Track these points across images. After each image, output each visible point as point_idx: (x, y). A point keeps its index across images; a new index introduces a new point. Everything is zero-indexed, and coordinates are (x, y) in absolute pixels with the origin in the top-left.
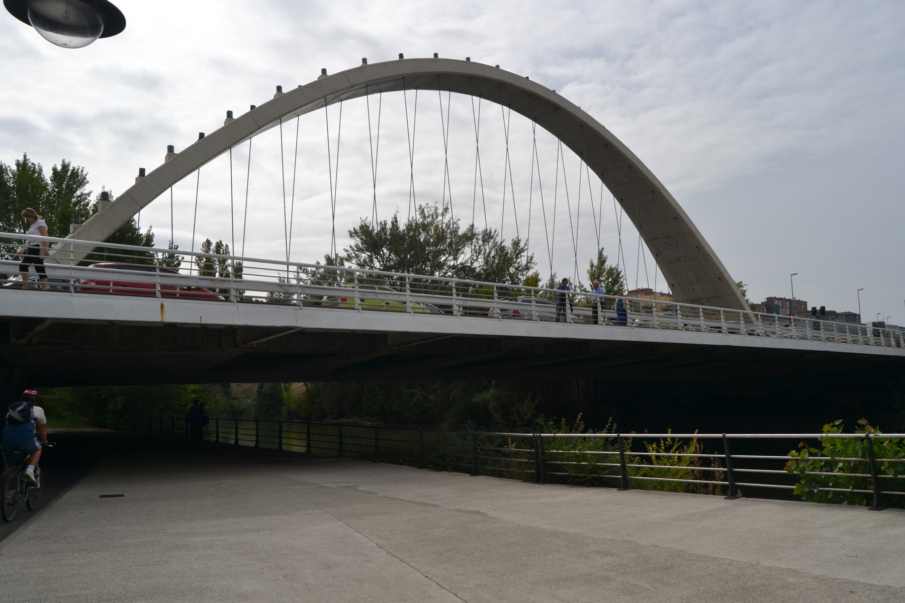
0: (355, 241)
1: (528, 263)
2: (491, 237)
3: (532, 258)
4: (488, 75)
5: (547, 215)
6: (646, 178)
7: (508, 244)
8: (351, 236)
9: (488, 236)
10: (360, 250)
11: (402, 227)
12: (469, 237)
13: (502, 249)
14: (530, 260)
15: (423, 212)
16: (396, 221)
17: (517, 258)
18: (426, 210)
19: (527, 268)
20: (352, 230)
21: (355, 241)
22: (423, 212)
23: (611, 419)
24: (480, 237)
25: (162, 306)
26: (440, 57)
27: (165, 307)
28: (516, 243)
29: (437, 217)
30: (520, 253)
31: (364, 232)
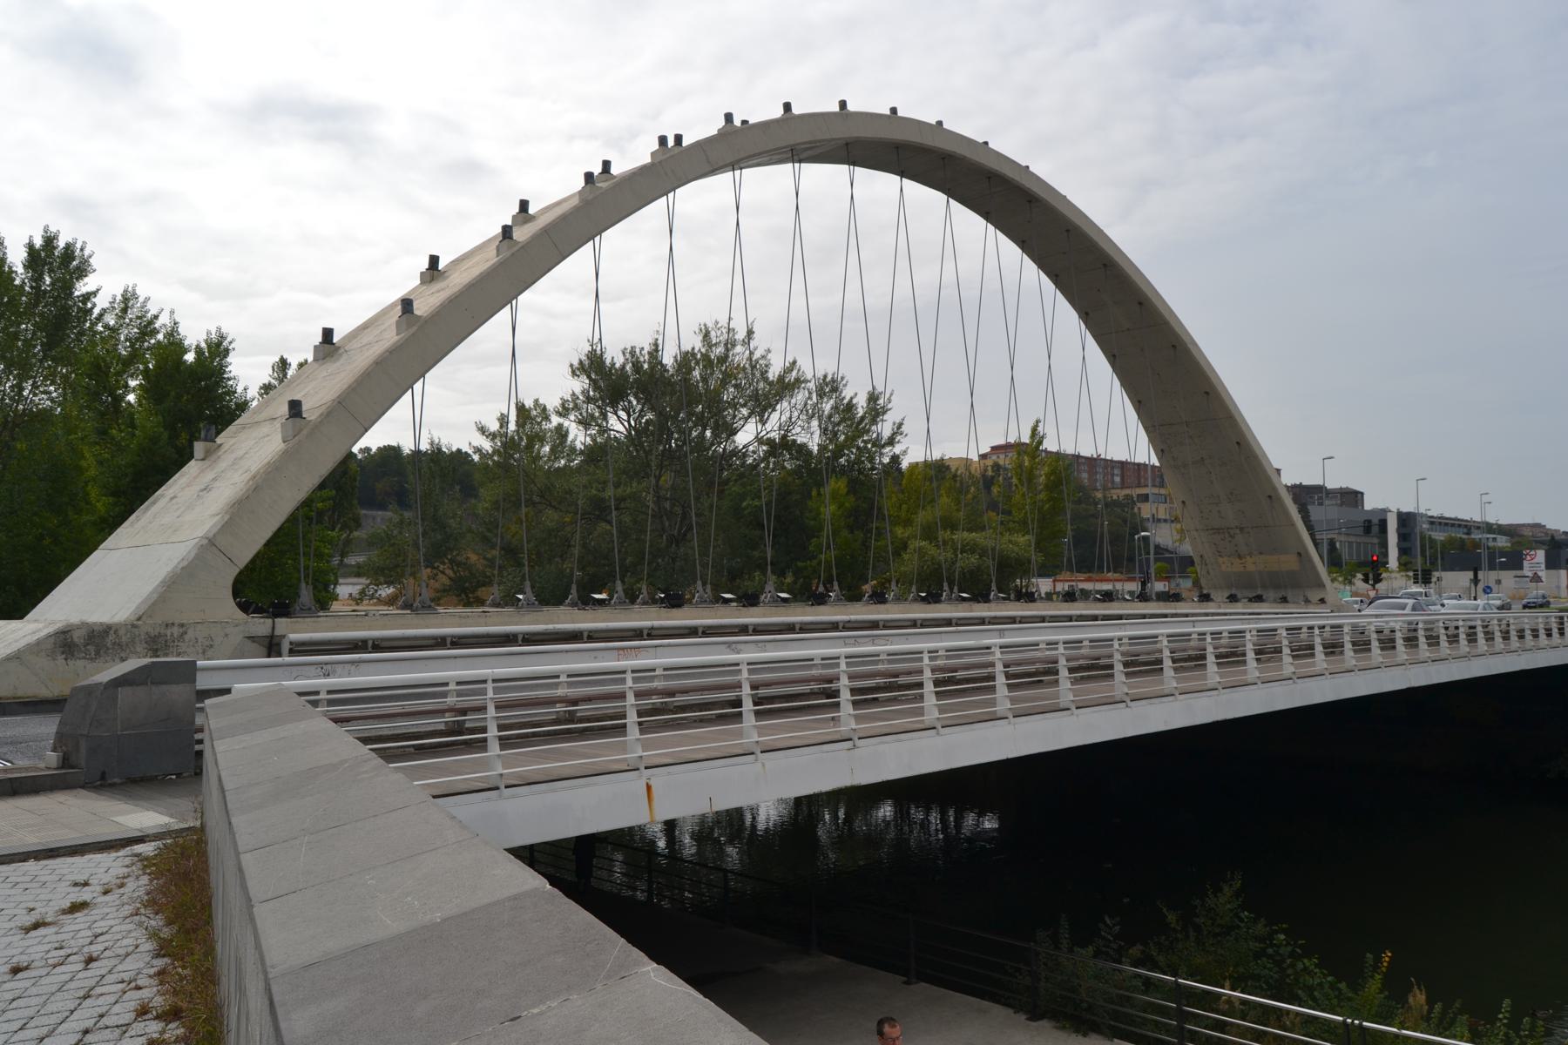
0: (579, 385)
1: (894, 434)
2: (835, 390)
3: (900, 425)
4: (929, 141)
5: (968, 366)
6: (1166, 323)
7: (861, 402)
8: (574, 373)
9: (829, 387)
10: (589, 400)
11: (668, 359)
12: (786, 386)
13: (850, 407)
14: (898, 428)
15: (707, 335)
16: (657, 350)
17: (874, 421)
18: (713, 334)
19: (891, 441)
20: (576, 363)
21: (579, 385)
22: (707, 335)
23: (1507, 1003)
24: (812, 385)
25: (649, 787)
26: (851, 107)
27: (654, 789)
28: (873, 398)
29: (734, 345)
30: (878, 415)
31: (593, 366)
